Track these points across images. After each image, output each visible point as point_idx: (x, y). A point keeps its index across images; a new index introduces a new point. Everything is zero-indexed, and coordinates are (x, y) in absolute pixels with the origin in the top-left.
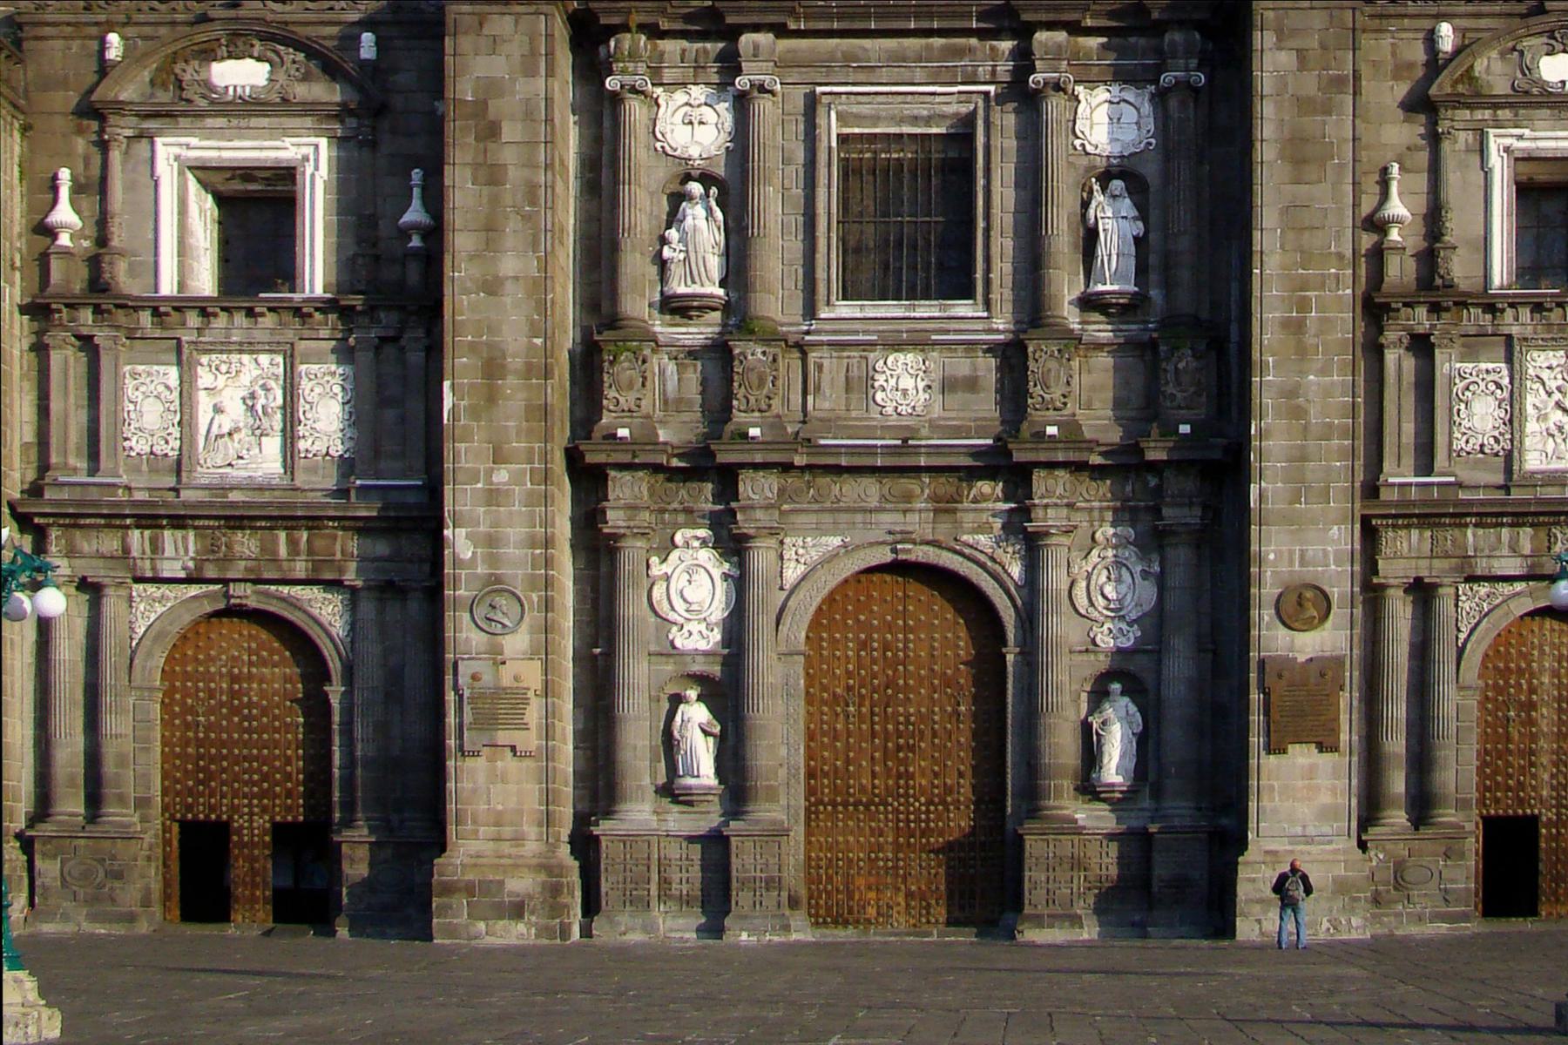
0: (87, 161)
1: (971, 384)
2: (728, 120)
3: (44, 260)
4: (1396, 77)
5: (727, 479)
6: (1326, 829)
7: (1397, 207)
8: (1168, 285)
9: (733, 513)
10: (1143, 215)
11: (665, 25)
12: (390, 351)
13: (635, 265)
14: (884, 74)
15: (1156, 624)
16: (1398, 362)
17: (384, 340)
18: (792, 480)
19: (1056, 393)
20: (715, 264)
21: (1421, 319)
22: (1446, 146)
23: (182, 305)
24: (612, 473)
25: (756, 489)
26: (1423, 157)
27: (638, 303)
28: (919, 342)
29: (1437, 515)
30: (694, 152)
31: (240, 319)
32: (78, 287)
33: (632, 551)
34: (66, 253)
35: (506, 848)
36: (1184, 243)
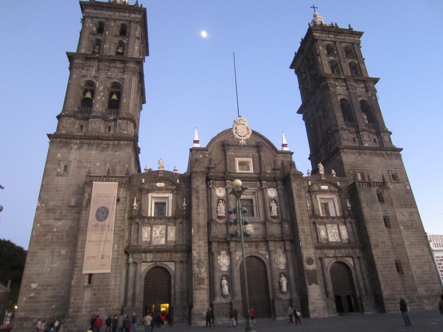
0: (138, 196)
1: (258, 228)
2: (225, 192)
8: (282, 215)
9: (229, 249)
10: (277, 205)
12: (181, 224)
13: (214, 212)
17: (180, 223)
19: (270, 230)
23: (151, 217)
24: (213, 242)
26: (309, 198)
30: (221, 196)
31: (160, 220)
33: (215, 254)
34: (135, 210)
36: (283, 209)
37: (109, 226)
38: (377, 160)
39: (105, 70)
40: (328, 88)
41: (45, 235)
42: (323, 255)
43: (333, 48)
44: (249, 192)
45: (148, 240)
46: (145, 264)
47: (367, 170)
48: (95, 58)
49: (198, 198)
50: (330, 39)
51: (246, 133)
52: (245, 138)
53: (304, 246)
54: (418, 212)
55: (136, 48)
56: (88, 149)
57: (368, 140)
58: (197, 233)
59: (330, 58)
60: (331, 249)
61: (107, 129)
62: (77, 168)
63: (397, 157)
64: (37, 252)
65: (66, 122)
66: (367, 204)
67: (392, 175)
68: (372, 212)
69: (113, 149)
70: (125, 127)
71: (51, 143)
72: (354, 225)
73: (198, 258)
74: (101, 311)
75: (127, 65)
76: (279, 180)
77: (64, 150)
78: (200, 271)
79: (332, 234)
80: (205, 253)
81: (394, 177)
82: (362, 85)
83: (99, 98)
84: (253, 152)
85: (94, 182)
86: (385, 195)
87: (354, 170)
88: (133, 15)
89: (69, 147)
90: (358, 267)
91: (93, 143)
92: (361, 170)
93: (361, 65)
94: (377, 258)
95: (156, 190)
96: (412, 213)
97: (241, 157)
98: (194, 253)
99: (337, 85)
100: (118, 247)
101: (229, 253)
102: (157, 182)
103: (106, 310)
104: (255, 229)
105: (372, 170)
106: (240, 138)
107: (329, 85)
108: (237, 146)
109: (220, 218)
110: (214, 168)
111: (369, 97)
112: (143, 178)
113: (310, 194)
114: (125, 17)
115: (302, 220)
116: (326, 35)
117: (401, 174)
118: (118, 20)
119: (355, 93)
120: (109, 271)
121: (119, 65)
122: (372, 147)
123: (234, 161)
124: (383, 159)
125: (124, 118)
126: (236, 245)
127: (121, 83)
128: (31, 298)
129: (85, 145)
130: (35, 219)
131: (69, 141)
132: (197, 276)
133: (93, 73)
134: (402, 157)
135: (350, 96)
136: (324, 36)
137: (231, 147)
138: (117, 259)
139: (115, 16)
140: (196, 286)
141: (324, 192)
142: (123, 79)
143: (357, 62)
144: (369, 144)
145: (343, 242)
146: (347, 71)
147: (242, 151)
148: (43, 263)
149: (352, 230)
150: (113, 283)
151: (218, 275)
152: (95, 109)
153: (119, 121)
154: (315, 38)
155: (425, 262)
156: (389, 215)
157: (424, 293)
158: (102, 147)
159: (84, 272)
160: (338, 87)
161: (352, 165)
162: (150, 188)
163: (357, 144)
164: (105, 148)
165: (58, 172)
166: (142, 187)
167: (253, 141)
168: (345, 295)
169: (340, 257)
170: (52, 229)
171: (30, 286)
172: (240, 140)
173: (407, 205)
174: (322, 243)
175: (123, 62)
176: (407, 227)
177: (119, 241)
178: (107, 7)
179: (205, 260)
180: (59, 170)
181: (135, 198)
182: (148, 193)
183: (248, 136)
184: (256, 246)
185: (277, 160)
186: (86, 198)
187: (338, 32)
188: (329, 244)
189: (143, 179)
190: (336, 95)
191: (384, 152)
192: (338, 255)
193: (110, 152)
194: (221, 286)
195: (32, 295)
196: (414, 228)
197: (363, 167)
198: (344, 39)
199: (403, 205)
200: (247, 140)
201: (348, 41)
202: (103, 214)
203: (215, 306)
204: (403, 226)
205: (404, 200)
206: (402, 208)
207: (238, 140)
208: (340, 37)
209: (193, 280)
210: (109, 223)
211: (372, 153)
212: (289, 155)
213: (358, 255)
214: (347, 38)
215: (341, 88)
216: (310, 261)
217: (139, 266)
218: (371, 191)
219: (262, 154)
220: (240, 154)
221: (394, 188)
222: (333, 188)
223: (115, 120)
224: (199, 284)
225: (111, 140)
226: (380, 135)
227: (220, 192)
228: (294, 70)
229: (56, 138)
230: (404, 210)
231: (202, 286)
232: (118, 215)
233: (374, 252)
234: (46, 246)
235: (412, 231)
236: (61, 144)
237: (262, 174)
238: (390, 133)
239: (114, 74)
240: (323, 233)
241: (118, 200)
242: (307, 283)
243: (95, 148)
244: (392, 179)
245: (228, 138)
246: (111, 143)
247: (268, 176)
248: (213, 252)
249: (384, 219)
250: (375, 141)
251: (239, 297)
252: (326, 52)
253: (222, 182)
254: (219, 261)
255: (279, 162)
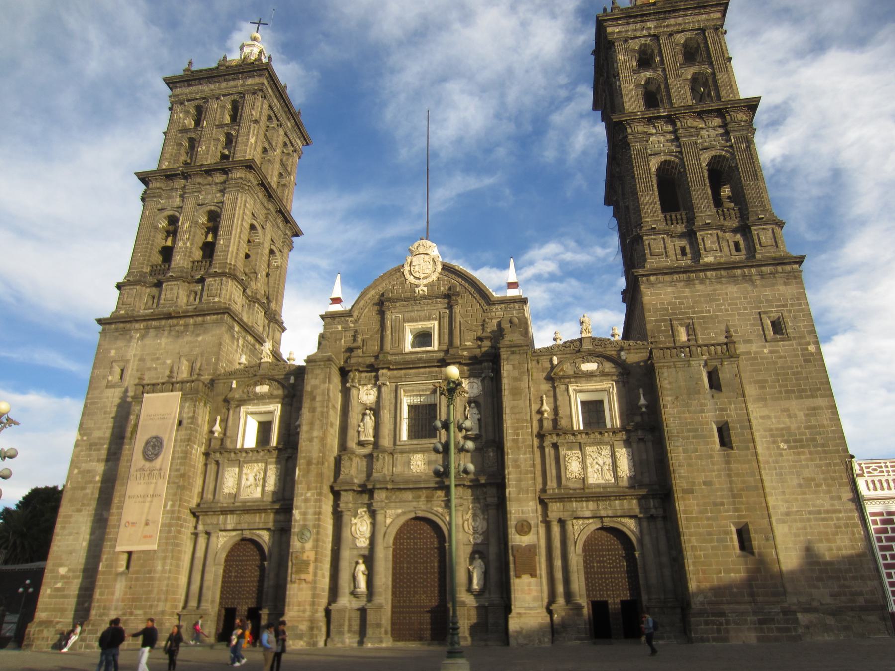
3: (210, 440)
4: (543, 372)
5: (371, 492)
6: (536, 605)
7: (546, 407)
10: (480, 413)
11: (361, 369)
13: (351, 433)
14: (415, 379)
15: (486, 534)
16: (549, 451)
18: (389, 494)
20: (371, 432)
21: (555, 439)
22: (558, 390)
24: (342, 493)
25: (380, 495)
26: (552, 393)
27: (352, 444)
28: (422, 451)
29: (564, 498)
32: (217, 447)
34: (216, 438)
35: (301, 614)
37: (160, 469)
38: (732, 290)
39: (193, 192)
40: (629, 145)
41: (83, 488)
42: (566, 514)
43: (653, 51)
44: (426, 390)
45: (234, 491)
46: (224, 533)
47: (703, 317)
48: (179, 174)
49: (313, 410)
50: (645, 32)
51: (429, 271)
52: (426, 281)
53: (512, 495)
54: (835, 407)
55: (252, 140)
56: (156, 336)
57: (716, 247)
58: (303, 476)
59: (643, 74)
60: (587, 501)
61: (192, 297)
62: (137, 371)
63: (788, 279)
64: (70, 516)
65: (128, 294)
66: (677, 398)
67: (773, 323)
68: (688, 415)
69: (193, 332)
70: (217, 289)
71: (103, 333)
72: (650, 445)
73: (301, 523)
74: (136, 615)
75: (230, 176)
76: (487, 361)
77: (120, 344)
78: (303, 548)
79: (597, 466)
80: (315, 514)
81: (778, 326)
82: (717, 121)
83: (181, 243)
84: (440, 306)
85: (145, 395)
86: (726, 373)
87: (671, 320)
88: (250, 81)
89: (128, 337)
90: (647, 539)
91: (164, 326)
92: (688, 318)
93: (719, 76)
94: (687, 519)
95: (253, 399)
96: (815, 408)
97: (416, 321)
98: (297, 514)
99: (652, 134)
100: (173, 506)
101: (373, 514)
102: (255, 384)
103: (145, 613)
104: (429, 463)
105: (717, 316)
106: (417, 282)
107: (630, 137)
108: (407, 299)
109: (361, 444)
110: (358, 348)
111: (731, 146)
112: (234, 379)
113: (553, 383)
114: (236, 87)
115: (515, 441)
116: (638, 26)
117: (794, 317)
118: (224, 96)
119: (696, 143)
120: (155, 547)
121: (219, 178)
122: (720, 264)
123: (398, 331)
124: (750, 288)
125: (216, 275)
126: (387, 498)
127: (219, 210)
128: (58, 590)
129: (151, 330)
130: (72, 462)
131: (128, 325)
132: (297, 557)
133: (177, 201)
134: (804, 276)
135: (681, 152)
136: (631, 29)
137: (398, 304)
138: (170, 525)
139: (220, 89)
140: (294, 576)
141: (589, 376)
142: (222, 203)
143: (709, 71)
144: (716, 257)
145: (620, 484)
146: (681, 93)
147: (419, 307)
148: (77, 533)
149: (645, 457)
150: (159, 568)
151: (346, 555)
152: (173, 264)
153: (208, 281)
154: (610, 37)
155: (839, 527)
156: (729, 420)
157: (828, 600)
158: (178, 331)
159: (118, 549)
160: (653, 138)
161: (667, 309)
162: (245, 397)
163: (687, 262)
164: (182, 332)
165: (108, 381)
166: (230, 395)
167: (443, 285)
168: (618, 601)
169: (607, 517)
170: (94, 476)
171: (58, 572)
172: (417, 286)
173: (805, 391)
174: (567, 488)
175: (225, 171)
176: (796, 443)
177: (175, 494)
178: (207, 78)
179: (314, 526)
180: (110, 378)
181: (219, 418)
182: (239, 406)
183: (434, 277)
184: (427, 497)
185: (492, 318)
186: (133, 422)
187: (664, 13)
188: (587, 490)
189: (234, 382)
190: (647, 157)
191: (753, 270)
192: (603, 513)
193: (188, 338)
194: (354, 578)
195: (59, 585)
196: (816, 446)
197: (694, 312)
198: (680, 24)
199: (793, 391)
200: (430, 286)
201: (691, 27)
202: (154, 448)
203: (334, 615)
204: (786, 442)
205: (797, 379)
206: (789, 398)
207: (414, 286)
208: (672, 21)
209: (290, 564)
210: (161, 465)
211: (722, 277)
212: (516, 305)
213: (653, 512)
214: (689, 19)
215: (662, 139)
216: (524, 528)
217: (213, 539)
218: (689, 366)
219: (457, 310)
220: (415, 314)
221: (771, 352)
222: (608, 367)
223: (202, 281)
224: (299, 571)
225: (192, 316)
226: (750, 232)
227: (366, 395)
228: (600, 112)
229: (110, 323)
230: (794, 404)
231: (303, 576)
232: (177, 449)
233: (680, 505)
234: (83, 505)
235: (811, 453)
236: (117, 334)
237: (452, 351)
238: (781, 224)
239: (210, 196)
240: (573, 467)
241: (180, 423)
242: (512, 573)
243: (166, 333)
244: (770, 332)
245: (394, 285)
246: (191, 321)
247: (465, 353)
248: (341, 512)
249: (720, 430)
250: (738, 248)
251: (385, 597)
252: (634, 64)
253: (374, 374)
254: (353, 529)
255: (495, 321)
